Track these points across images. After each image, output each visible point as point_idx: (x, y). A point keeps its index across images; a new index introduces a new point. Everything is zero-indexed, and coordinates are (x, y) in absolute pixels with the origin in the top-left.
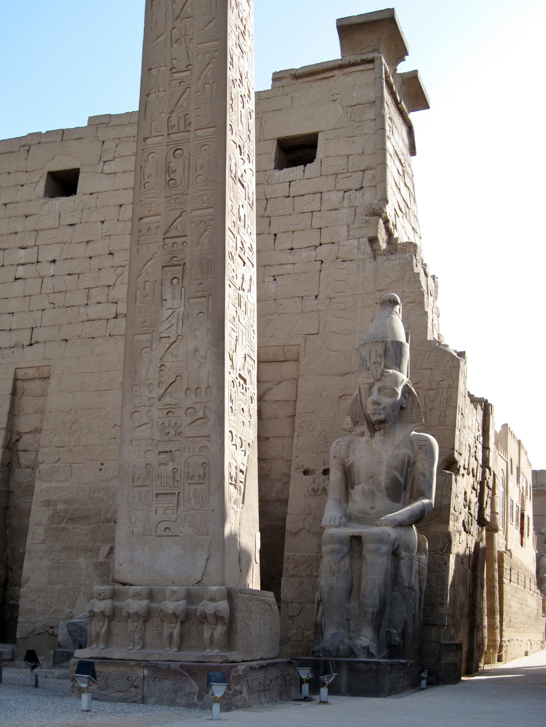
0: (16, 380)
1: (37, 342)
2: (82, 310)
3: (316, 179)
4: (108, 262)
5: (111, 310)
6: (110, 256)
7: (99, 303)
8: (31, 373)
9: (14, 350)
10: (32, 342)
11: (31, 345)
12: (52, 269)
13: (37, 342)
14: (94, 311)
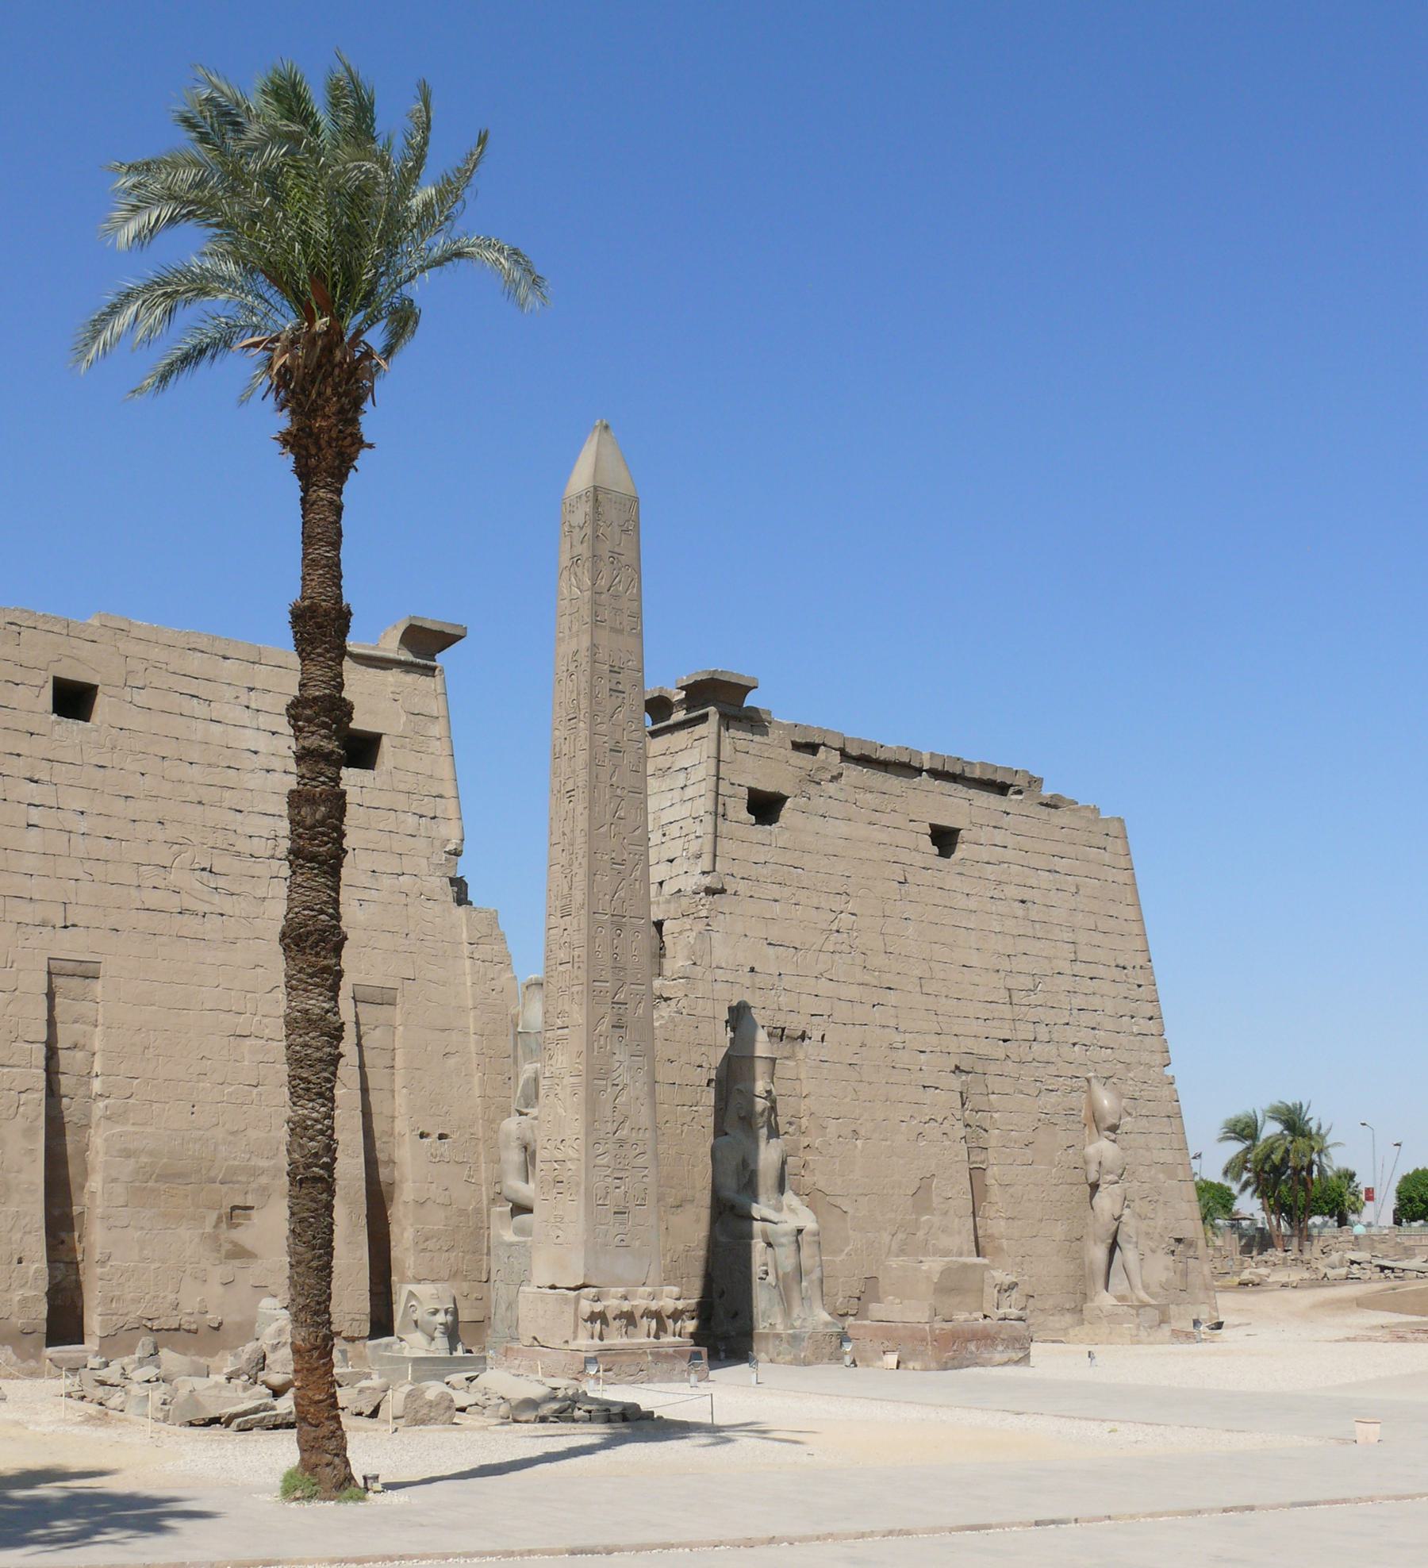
0: (49, 973)
1: (73, 925)
2: (134, 892)
3: (387, 793)
4: (160, 834)
5: (174, 903)
6: (161, 826)
7: (154, 887)
8: (70, 967)
9: (41, 929)
10: (68, 924)
11: (66, 927)
12: (83, 825)
13: (73, 925)
14: (153, 899)
